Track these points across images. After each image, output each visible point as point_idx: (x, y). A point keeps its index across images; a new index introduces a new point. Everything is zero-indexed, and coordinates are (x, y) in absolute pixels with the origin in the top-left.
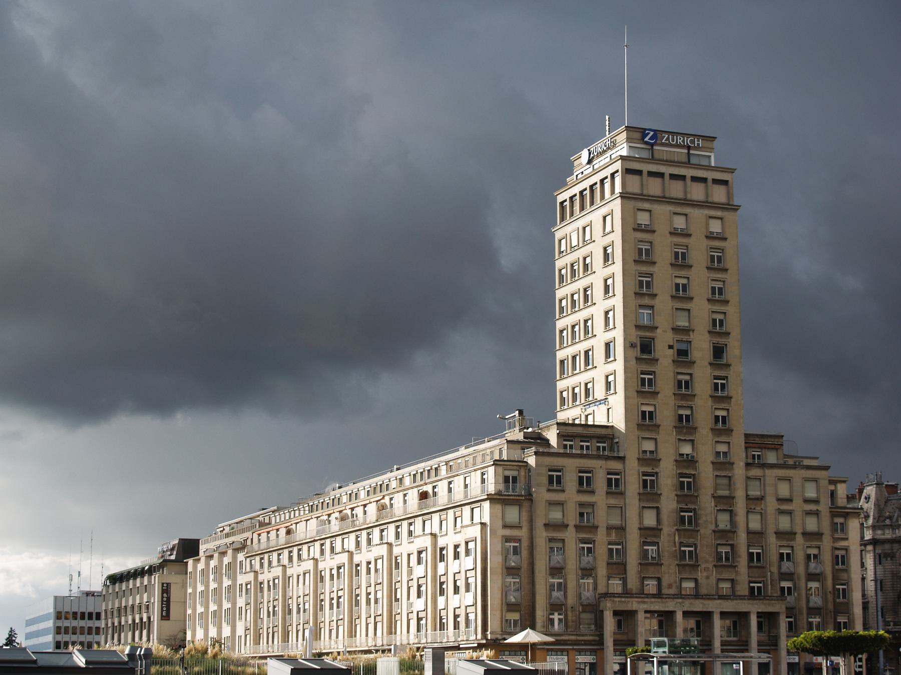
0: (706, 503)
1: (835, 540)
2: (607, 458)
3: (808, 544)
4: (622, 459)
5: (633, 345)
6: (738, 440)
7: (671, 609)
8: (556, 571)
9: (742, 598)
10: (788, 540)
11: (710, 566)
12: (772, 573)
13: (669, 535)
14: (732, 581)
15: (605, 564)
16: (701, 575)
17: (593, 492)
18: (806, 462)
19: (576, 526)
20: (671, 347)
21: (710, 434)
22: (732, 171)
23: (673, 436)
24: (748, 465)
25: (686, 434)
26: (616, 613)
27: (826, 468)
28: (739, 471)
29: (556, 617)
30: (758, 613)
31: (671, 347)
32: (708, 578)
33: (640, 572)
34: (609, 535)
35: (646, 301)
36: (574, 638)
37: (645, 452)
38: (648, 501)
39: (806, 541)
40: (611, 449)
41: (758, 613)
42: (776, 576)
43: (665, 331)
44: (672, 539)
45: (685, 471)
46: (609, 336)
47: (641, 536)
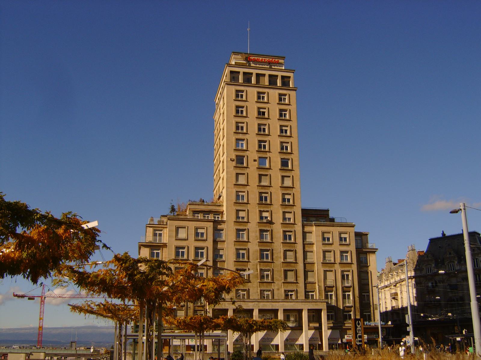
0: (279, 247)
5: (232, 160)
7: (251, 308)
10: (329, 267)
13: (253, 265)
16: (274, 287)
20: (255, 161)
21: (280, 207)
25: (264, 207)
30: (308, 310)
31: (255, 161)
38: (240, 245)
39: (341, 267)
41: (308, 310)
43: (252, 152)
44: (255, 267)
45: (263, 228)
47: (235, 265)
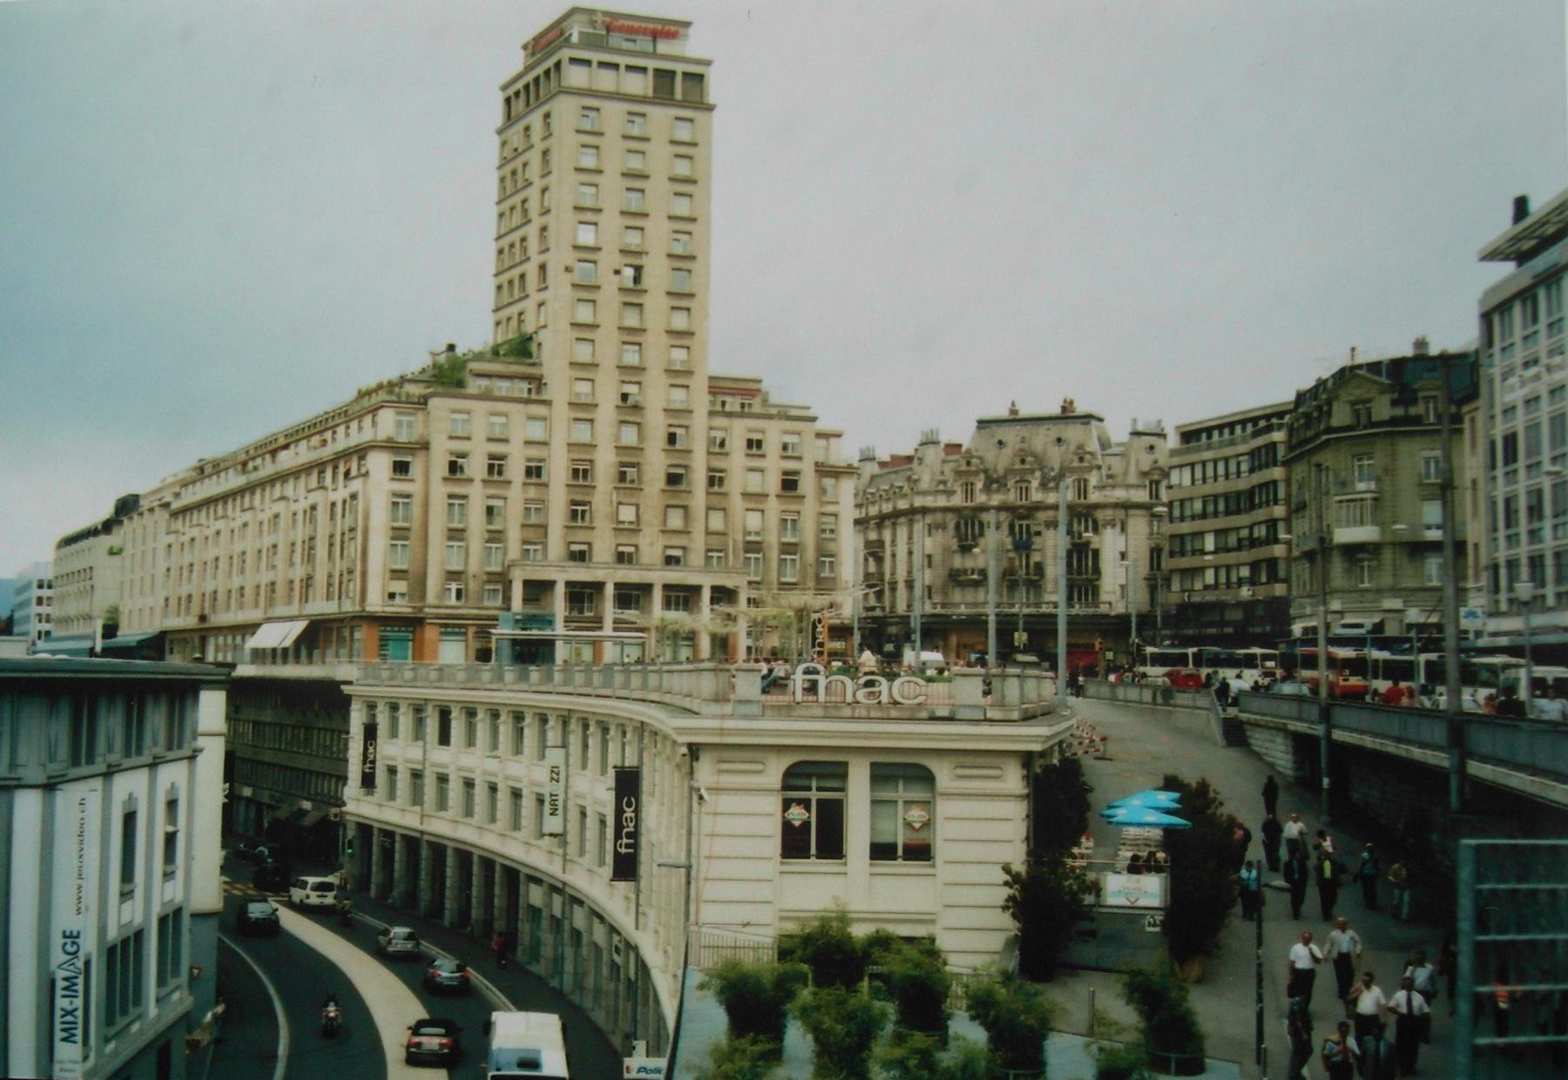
1: (822, 503)
2: (527, 401)
3: (784, 507)
4: (547, 403)
6: (700, 384)
7: (601, 579)
8: (456, 534)
9: (694, 570)
11: (656, 530)
12: (735, 541)
14: (684, 548)
15: (518, 526)
17: (506, 441)
18: (794, 412)
19: (484, 481)
20: (617, 272)
22: (708, 63)
23: (616, 376)
24: (712, 414)
26: (527, 584)
27: (814, 419)
28: (699, 422)
29: (454, 586)
32: (651, 544)
33: (566, 536)
34: (525, 492)
35: (589, 217)
36: (475, 612)
37: (578, 394)
40: (539, 392)
42: (741, 546)
46: (542, 258)
